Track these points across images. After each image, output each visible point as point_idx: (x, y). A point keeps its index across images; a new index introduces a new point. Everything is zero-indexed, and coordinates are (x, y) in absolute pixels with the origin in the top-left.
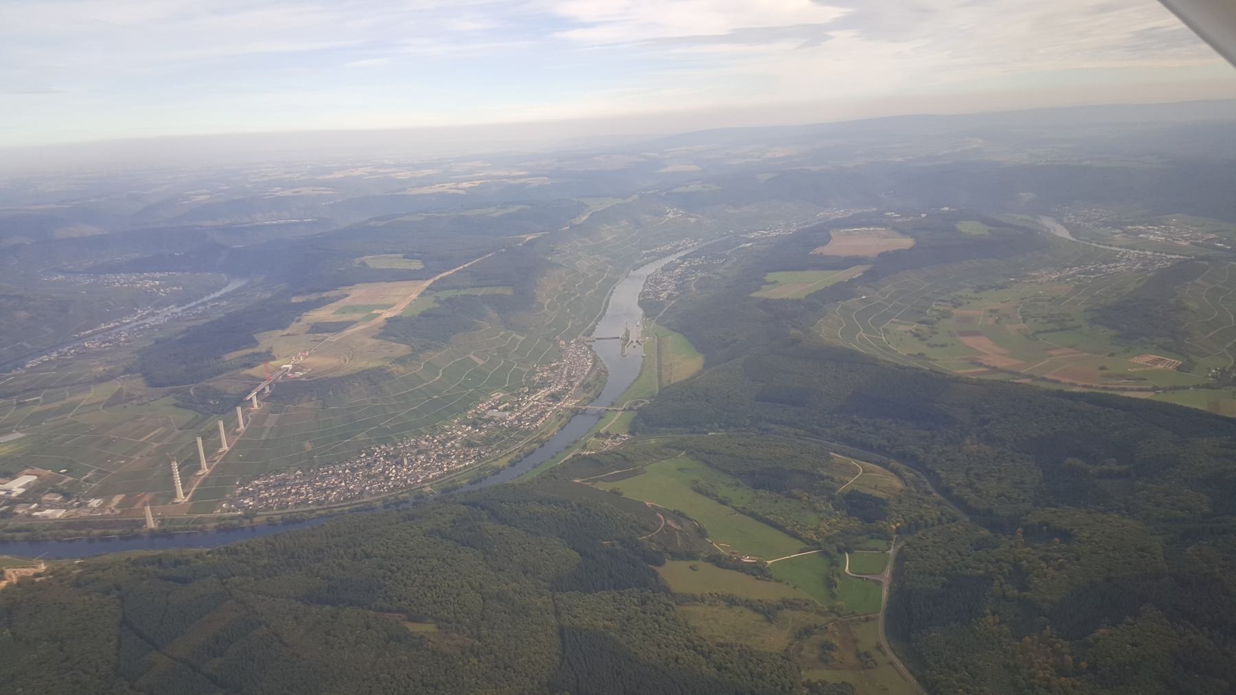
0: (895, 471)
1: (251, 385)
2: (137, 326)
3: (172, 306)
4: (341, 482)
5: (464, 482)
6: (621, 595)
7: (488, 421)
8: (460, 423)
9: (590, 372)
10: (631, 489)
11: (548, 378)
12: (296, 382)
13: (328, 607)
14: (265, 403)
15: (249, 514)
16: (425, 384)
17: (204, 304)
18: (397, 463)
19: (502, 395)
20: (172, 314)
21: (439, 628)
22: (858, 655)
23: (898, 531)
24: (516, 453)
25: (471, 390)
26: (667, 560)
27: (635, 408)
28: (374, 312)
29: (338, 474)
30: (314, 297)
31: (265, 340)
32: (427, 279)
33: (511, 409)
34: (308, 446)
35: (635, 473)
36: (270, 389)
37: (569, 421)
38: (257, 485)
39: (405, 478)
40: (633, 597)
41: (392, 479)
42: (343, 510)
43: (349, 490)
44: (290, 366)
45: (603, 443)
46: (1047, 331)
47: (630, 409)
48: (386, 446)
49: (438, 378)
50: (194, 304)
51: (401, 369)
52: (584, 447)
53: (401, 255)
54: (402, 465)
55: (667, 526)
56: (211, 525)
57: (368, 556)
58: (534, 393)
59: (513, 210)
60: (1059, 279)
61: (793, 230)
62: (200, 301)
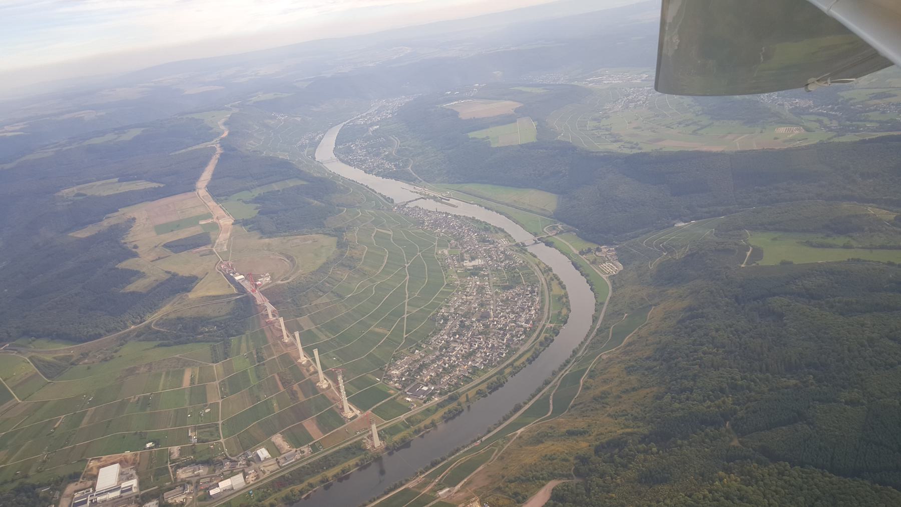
1: (229, 302)
28: (202, 222)
38: (403, 375)
53: (116, 180)
56: (437, 416)
59: (137, 132)
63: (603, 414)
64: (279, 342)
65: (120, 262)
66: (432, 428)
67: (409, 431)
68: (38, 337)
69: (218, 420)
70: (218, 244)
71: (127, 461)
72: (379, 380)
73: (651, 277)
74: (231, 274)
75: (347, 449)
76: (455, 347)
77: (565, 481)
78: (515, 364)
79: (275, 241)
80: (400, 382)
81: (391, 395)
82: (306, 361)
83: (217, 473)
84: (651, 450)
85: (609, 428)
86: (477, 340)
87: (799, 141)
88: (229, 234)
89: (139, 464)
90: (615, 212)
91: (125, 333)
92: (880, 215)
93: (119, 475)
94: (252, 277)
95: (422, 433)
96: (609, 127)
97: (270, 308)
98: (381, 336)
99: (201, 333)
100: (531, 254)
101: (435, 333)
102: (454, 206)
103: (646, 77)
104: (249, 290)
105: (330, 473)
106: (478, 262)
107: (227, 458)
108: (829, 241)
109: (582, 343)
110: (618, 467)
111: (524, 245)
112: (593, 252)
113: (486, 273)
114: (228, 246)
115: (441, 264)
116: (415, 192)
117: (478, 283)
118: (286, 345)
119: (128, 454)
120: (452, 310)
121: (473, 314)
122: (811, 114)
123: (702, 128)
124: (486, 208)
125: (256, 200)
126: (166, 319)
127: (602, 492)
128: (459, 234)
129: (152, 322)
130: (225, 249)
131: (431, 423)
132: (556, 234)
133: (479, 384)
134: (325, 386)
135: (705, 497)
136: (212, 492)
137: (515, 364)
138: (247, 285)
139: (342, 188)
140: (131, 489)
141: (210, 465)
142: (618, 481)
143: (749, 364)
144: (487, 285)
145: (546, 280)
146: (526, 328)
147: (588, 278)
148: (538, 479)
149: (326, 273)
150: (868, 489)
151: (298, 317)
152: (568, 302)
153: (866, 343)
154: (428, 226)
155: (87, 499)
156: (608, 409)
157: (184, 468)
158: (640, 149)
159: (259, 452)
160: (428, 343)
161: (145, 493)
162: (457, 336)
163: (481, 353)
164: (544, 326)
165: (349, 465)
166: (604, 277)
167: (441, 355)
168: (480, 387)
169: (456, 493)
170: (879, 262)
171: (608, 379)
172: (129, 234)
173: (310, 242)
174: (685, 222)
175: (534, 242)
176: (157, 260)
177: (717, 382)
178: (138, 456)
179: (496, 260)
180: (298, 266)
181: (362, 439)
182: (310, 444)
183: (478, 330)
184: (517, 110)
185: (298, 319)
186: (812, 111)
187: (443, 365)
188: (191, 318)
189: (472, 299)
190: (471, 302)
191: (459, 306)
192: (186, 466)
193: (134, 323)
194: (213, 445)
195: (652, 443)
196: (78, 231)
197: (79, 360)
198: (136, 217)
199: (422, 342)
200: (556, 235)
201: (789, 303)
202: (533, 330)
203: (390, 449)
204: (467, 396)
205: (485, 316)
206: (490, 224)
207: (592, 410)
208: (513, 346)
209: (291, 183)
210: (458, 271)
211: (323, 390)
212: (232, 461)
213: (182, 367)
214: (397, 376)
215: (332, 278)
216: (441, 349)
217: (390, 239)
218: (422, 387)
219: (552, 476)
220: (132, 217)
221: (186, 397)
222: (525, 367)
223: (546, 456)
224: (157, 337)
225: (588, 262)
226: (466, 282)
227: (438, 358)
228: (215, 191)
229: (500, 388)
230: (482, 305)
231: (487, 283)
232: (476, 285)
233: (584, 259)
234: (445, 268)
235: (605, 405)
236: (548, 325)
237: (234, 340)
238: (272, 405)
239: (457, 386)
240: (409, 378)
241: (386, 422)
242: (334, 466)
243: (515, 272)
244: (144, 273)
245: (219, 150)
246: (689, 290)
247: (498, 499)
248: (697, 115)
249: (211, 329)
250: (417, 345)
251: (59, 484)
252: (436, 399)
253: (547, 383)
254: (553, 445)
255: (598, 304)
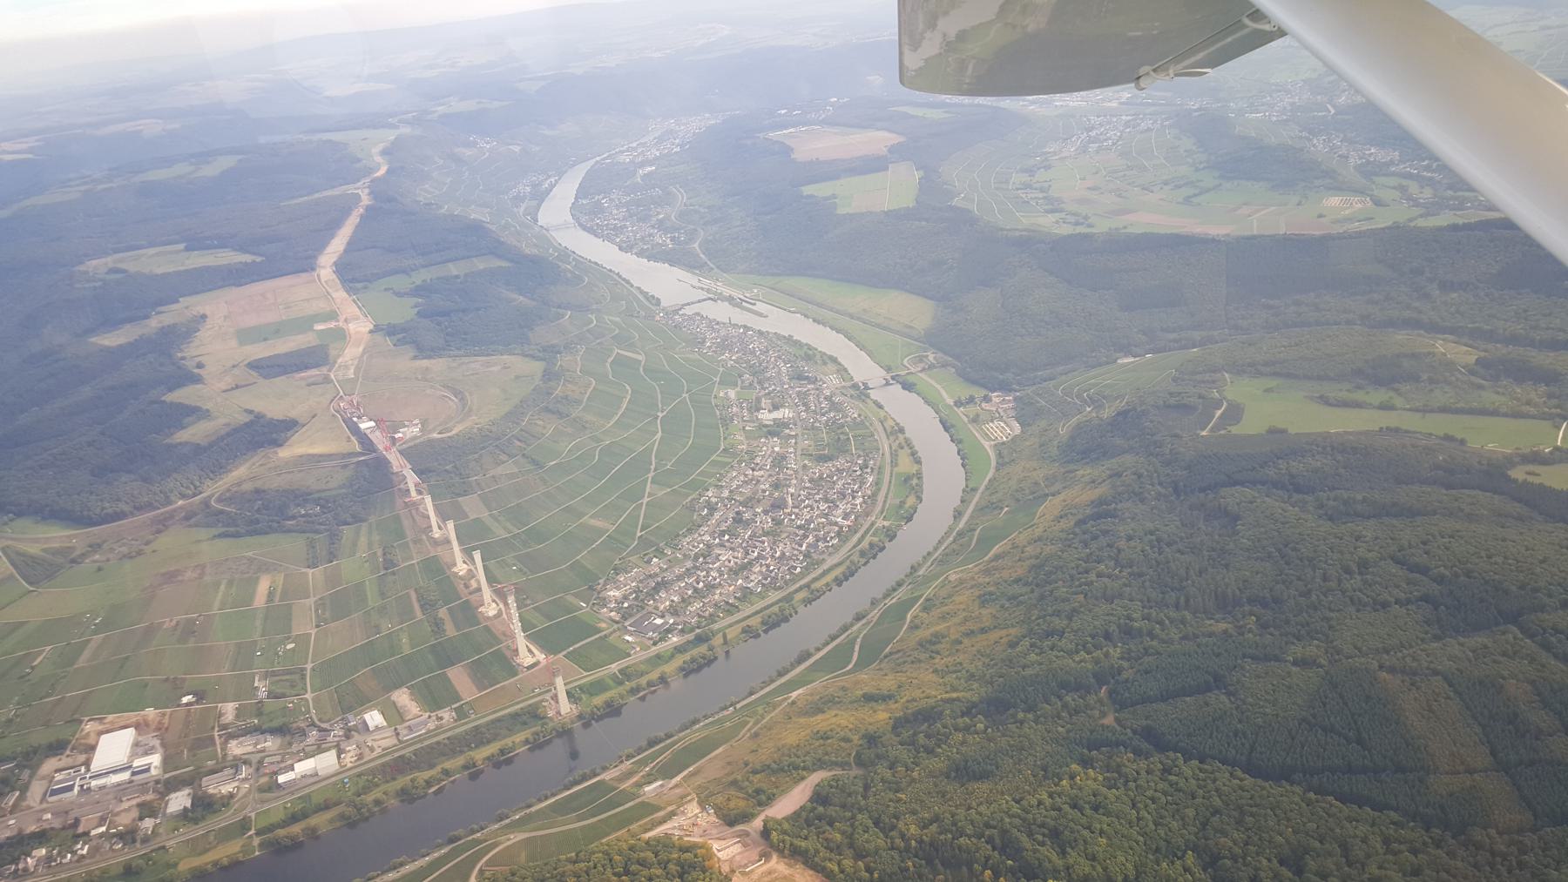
1: (345, 466)
28: (319, 327)
38: (625, 598)
56: (669, 668)
63: (927, 669)
64: (424, 537)
65: (170, 390)
66: (660, 686)
67: (621, 689)
68: (20, 514)
69: (306, 663)
70: (340, 367)
71: (147, 725)
72: (584, 605)
73: (1058, 447)
74: (355, 419)
75: (515, 716)
76: (719, 555)
77: (837, 773)
78: (813, 586)
79: (437, 365)
80: (618, 610)
81: (600, 631)
82: (465, 571)
83: (295, 748)
84: (975, 726)
85: (928, 691)
86: (758, 544)
87: (1359, 221)
88: (361, 349)
89: (167, 729)
90: (1021, 336)
91: (167, 512)
92: (1453, 356)
93: (132, 747)
94: (388, 425)
95: (641, 694)
96: (1046, 185)
97: (412, 479)
98: (601, 532)
99: (293, 518)
100: (875, 402)
101: (690, 531)
102: (761, 315)
103: (1128, 99)
104: (381, 447)
105: (481, 754)
106: (785, 413)
107: (313, 724)
108: (1359, 396)
109: (929, 554)
110: (919, 753)
111: (867, 388)
112: (976, 403)
113: (793, 433)
114: (356, 372)
115: (721, 414)
116: (699, 288)
117: (777, 449)
118: (436, 543)
119: (150, 712)
120: (726, 493)
121: (759, 501)
122: (1393, 174)
123: (1200, 194)
124: (814, 321)
125: (417, 291)
126: (236, 492)
127: (888, 791)
128: (760, 365)
129: (213, 495)
130: (351, 374)
131: (659, 678)
132: (923, 370)
133: (749, 617)
134: (492, 613)
135: (1040, 803)
136: (282, 779)
137: (813, 586)
138: (379, 440)
139: (569, 275)
140: (148, 770)
141: (285, 736)
142: (915, 774)
143: (1161, 595)
144: (791, 453)
145: (891, 448)
146: (841, 527)
147: (960, 446)
148: (797, 768)
149: (517, 424)
150: (1297, 799)
151: (459, 495)
152: (920, 486)
153: (1355, 568)
154: (710, 347)
155: (74, 784)
156: (937, 661)
157: (241, 739)
158: (1090, 226)
159: (367, 717)
160: (675, 548)
161: (170, 777)
162: (727, 537)
163: (761, 565)
164: (872, 524)
165: (513, 742)
166: (986, 444)
167: (696, 568)
168: (751, 622)
169: (671, 789)
170: (1431, 434)
171: (948, 614)
172: (191, 342)
173: (495, 369)
174: (1135, 357)
175: (884, 382)
176: (233, 389)
177: (1103, 623)
178: (167, 717)
179: (815, 411)
180: (470, 410)
181: (542, 701)
182: (453, 706)
183: (763, 528)
184: (892, 150)
185: (460, 499)
186: (1394, 169)
187: (695, 584)
188: (278, 491)
189: (762, 476)
190: (758, 481)
191: (738, 487)
192: (245, 736)
193: (183, 496)
194: (293, 702)
195: (979, 716)
196: (105, 335)
197: (83, 555)
198: (208, 313)
199: (666, 544)
200: (921, 371)
201: (1254, 497)
202: (853, 530)
203: (585, 718)
204: (725, 636)
205: (778, 505)
206: (816, 350)
207: (913, 662)
208: (815, 556)
209: (480, 264)
210: (747, 428)
211: (488, 618)
212: (321, 730)
213: (254, 573)
214: (616, 600)
215: (527, 432)
216: (696, 557)
217: (638, 369)
218: (655, 619)
219: (820, 764)
220: (202, 312)
221: (258, 623)
222: (830, 590)
223: (818, 732)
224: (219, 521)
225: (966, 419)
226: (758, 446)
227: (688, 573)
228: (351, 274)
229: (783, 624)
230: (776, 486)
231: (791, 450)
232: (773, 452)
233: (961, 415)
234: (726, 421)
235: (933, 655)
236: (880, 523)
237: (347, 532)
238: (400, 640)
239: (712, 618)
240: (636, 603)
241: (585, 674)
242: (489, 742)
243: (842, 433)
244: (208, 411)
245: (366, 200)
246: (1108, 472)
247: (729, 799)
248: (1197, 170)
249: (311, 512)
250: (656, 550)
251: (31, 758)
252: (675, 639)
253: (859, 617)
254: (836, 715)
255: (968, 489)
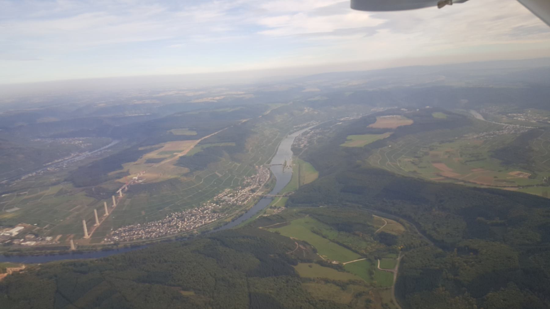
0: (402, 223)
2: (71, 161)
3: (87, 152)
4: (157, 229)
5: (212, 228)
6: (277, 278)
7: (223, 201)
8: (210, 203)
9: (269, 179)
10: (284, 231)
11: (250, 182)
12: (139, 184)
13: (147, 284)
14: (125, 194)
15: (116, 243)
16: (196, 185)
17: (101, 151)
18: (182, 221)
19: (229, 190)
20: (87, 155)
21: (195, 293)
22: (382, 305)
23: (402, 250)
24: (235, 215)
25: (216, 188)
26: (298, 263)
27: (288, 195)
28: (175, 154)
29: (156, 226)
30: (149, 147)
31: (127, 167)
32: (198, 139)
33: (233, 196)
34: (143, 213)
35: (286, 224)
36: (128, 188)
37: (259, 201)
38: (120, 230)
39: (186, 227)
40: (283, 279)
41: (180, 227)
42: (158, 242)
43: (160, 232)
44: (136, 178)
45: (273, 211)
46: (471, 161)
47: (286, 196)
48: (178, 212)
49: (201, 182)
50: (96, 151)
51: (185, 179)
52: (265, 213)
53: (187, 129)
54: (184, 221)
55: (299, 247)
57: (166, 262)
58: (243, 189)
60: (477, 138)
61: (360, 117)
62: (99, 150)
